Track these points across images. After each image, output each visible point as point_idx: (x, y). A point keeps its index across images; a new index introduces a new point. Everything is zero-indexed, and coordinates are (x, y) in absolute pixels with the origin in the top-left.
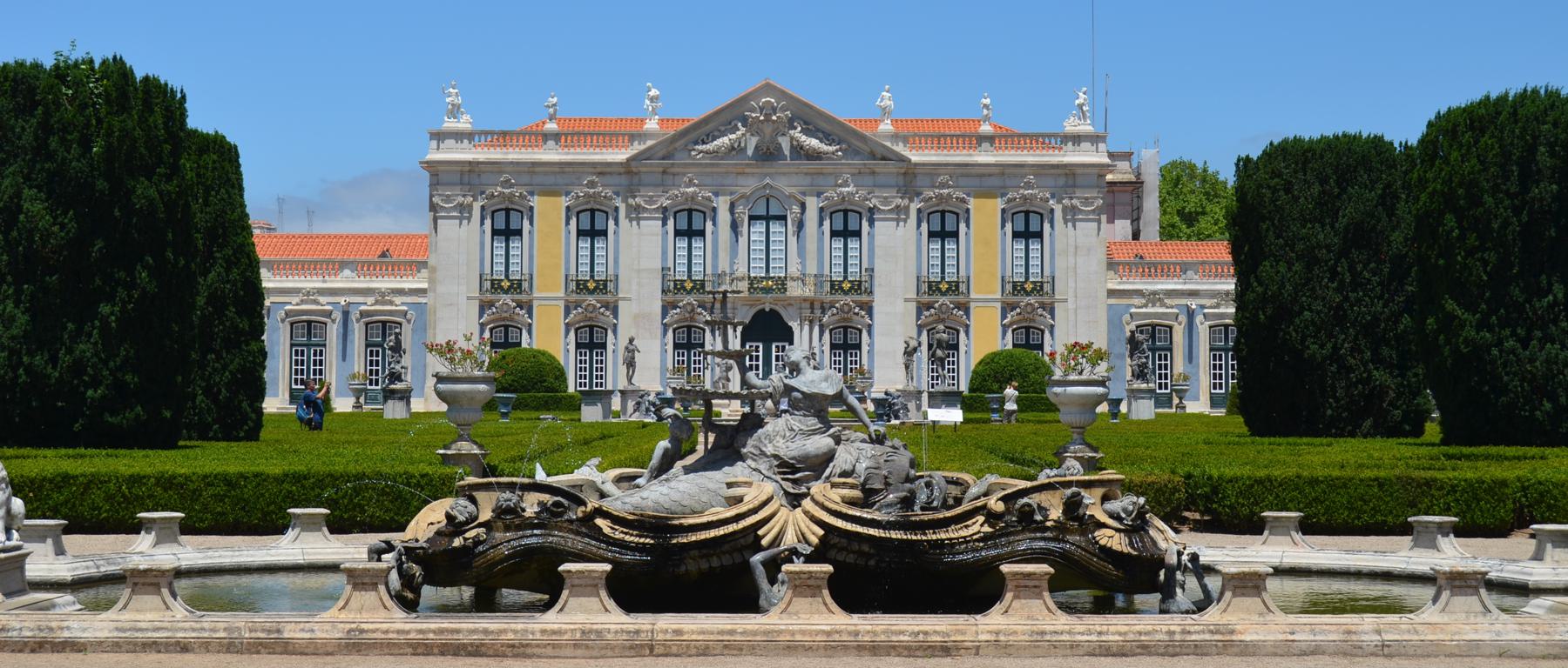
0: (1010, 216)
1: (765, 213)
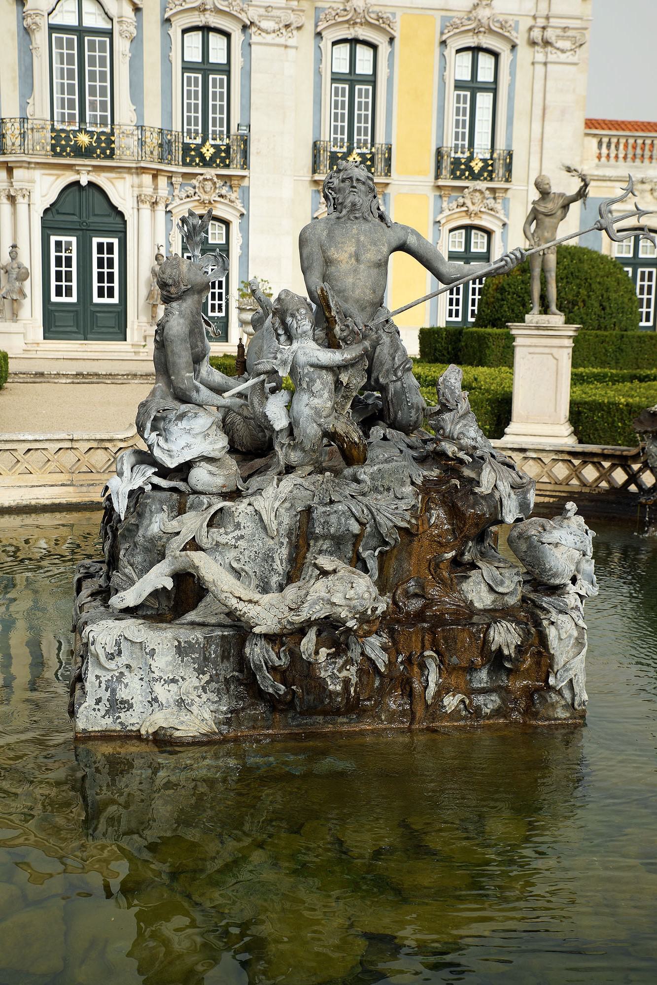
0: (454, 52)
1: (77, 24)
